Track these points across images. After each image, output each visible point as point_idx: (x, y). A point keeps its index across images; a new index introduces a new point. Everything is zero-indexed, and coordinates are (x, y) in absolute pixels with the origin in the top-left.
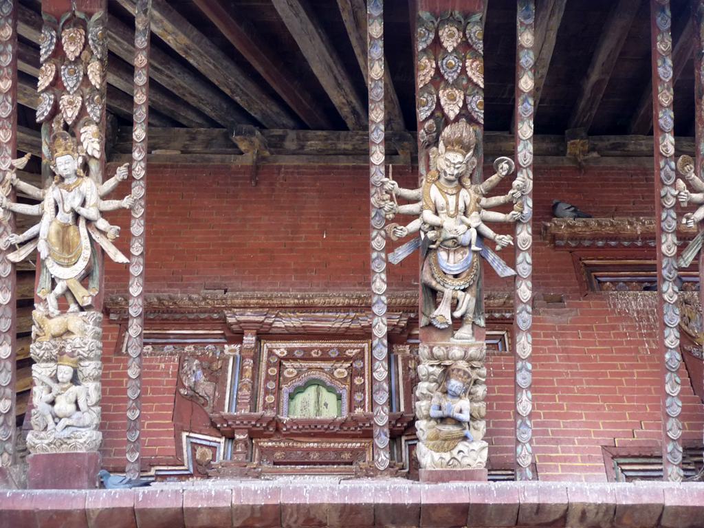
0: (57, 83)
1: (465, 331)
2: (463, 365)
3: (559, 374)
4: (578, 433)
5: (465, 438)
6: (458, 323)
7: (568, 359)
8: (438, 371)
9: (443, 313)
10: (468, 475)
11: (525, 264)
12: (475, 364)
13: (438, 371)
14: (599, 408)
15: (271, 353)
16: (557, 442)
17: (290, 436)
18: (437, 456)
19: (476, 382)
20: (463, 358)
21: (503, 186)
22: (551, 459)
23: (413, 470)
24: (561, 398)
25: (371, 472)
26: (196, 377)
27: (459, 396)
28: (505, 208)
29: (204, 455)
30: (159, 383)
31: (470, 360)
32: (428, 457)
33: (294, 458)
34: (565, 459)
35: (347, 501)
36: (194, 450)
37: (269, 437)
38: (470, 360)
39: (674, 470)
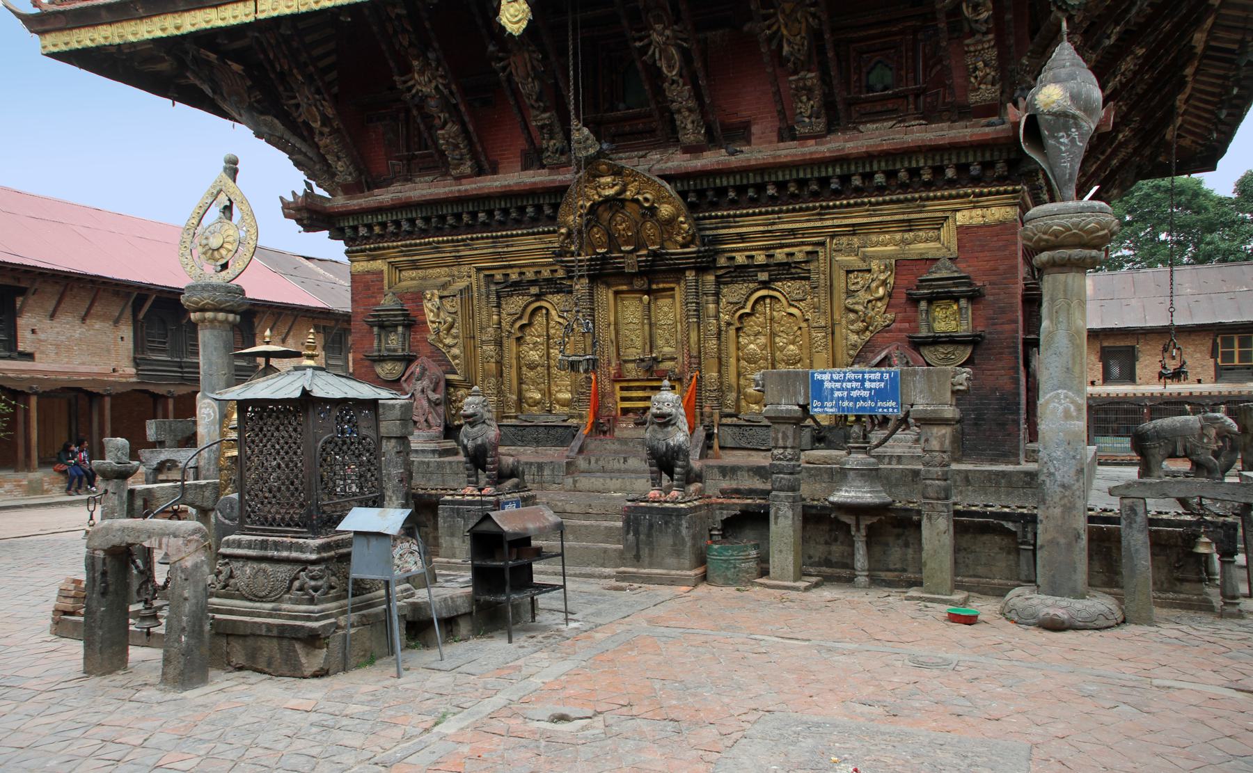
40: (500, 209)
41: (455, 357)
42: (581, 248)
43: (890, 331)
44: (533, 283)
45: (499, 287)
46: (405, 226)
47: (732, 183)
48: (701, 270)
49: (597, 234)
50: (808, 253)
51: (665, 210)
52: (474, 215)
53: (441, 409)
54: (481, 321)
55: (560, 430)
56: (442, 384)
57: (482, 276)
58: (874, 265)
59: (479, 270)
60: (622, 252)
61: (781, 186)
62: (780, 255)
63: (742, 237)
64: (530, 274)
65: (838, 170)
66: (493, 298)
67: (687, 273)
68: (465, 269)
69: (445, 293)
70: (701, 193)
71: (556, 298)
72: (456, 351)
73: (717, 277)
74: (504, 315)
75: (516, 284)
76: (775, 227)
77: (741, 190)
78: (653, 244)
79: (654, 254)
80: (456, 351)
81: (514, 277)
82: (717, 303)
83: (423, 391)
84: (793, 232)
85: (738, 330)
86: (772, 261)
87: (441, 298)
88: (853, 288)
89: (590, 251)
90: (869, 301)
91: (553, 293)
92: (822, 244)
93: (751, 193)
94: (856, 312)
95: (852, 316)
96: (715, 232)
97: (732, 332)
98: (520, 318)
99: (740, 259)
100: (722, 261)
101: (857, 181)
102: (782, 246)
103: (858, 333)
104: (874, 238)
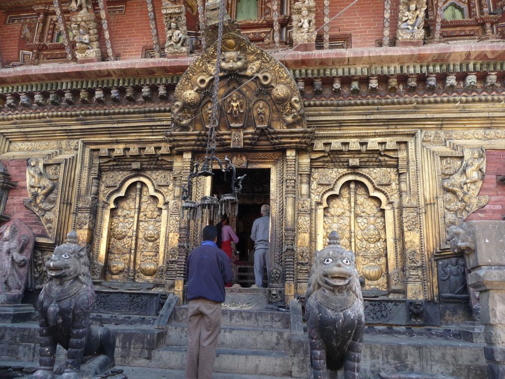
1: (84, 11)
2: (83, 23)
3: (136, 21)
4: (137, 42)
5: (89, 48)
6: (80, 8)
7: (141, 14)
8: (76, 26)
10: (91, 61)
12: (87, 23)
13: (76, 26)
14: (145, 32)
15: (52, 20)
16: (129, 46)
17: (51, 49)
18: (80, 55)
19: (90, 29)
20: (82, 21)
22: (126, 52)
23: (74, 59)
24: (135, 30)
25: (68, 62)
26: (26, 31)
27: (83, 35)
29: (27, 58)
30: (15, 34)
31: (85, 22)
32: (79, 56)
33: (53, 57)
34: (130, 52)
35: (44, 72)
36: (24, 56)
37: (45, 50)
38: (85, 22)
39: (157, 54)
40: (117, 88)
41: (49, 221)
42: (191, 123)
43: (484, 212)
44: (136, 158)
45: (102, 161)
46: (23, 99)
47: (340, 73)
48: (300, 151)
50: (399, 143)
52: (91, 92)
53: (23, 271)
54: (79, 189)
55: (144, 298)
56: (31, 246)
57: (87, 150)
58: (467, 155)
60: (230, 128)
61: (384, 79)
62: (373, 144)
63: (341, 124)
64: (134, 150)
65: (438, 69)
66: (95, 170)
67: (289, 153)
68: (73, 143)
69: (51, 162)
70: (309, 82)
71: (154, 175)
72: (49, 215)
73: (311, 159)
74: (103, 188)
75: (118, 158)
76: (372, 117)
77: (346, 81)
78: (262, 122)
79: (263, 132)
82: (309, 183)
84: (387, 122)
85: (325, 209)
86: (364, 148)
88: (446, 172)
89: (198, 126)
90: (465, 183)
91: (150, 169)
92: (413, 135)
93: (355, 85)
94: (454, 193)
95: (449, 196)
96: (317, 118)
97: (320, 212)
99: (336, 144)
100: (319, 145)
101: (451, 80)
102: (375, 136)
103: (456, 212)
104: (460, 132)
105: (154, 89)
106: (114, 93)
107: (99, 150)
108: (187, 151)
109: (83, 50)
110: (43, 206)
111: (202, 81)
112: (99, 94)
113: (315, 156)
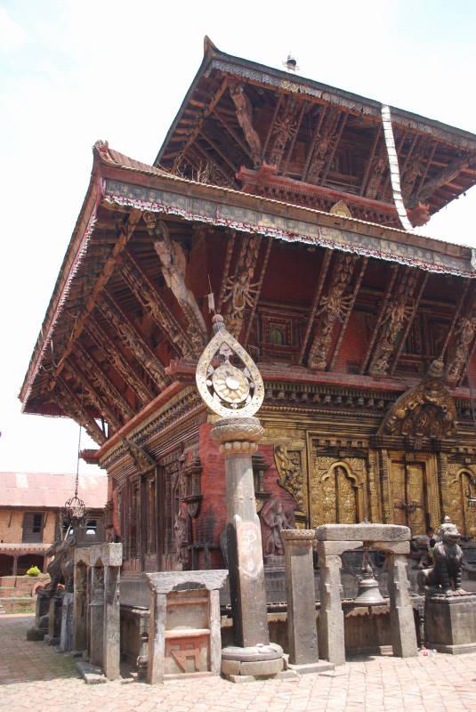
0: (246, 256)
9: (326, 330)
11: (347, 320)
21: (349, 300)
28: (347, 306)
41: (300, 498)
44: (343, 449)
45: (319, 448)
48: (448, 452)
49: (408, 424)
51: (449, 416)
59: (311, 435)
64: (344, 443)
68: (300, 433)
72: (300, 493)
75: (332, 448)
80: (300, 493)
81: (333, 443)
83: (283, 524)
87: (288, 452)
91: (349, 458)
98: (326, 473)
99: (461, 450)
105: (366, 401)
106: (339, 400)
107: (318, 440)
108: (384, 448)
109: (317, 362)
110: (296, 486)
111: (412, 405)
112: (328, 399)
113: (449, 456)
